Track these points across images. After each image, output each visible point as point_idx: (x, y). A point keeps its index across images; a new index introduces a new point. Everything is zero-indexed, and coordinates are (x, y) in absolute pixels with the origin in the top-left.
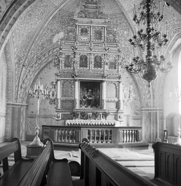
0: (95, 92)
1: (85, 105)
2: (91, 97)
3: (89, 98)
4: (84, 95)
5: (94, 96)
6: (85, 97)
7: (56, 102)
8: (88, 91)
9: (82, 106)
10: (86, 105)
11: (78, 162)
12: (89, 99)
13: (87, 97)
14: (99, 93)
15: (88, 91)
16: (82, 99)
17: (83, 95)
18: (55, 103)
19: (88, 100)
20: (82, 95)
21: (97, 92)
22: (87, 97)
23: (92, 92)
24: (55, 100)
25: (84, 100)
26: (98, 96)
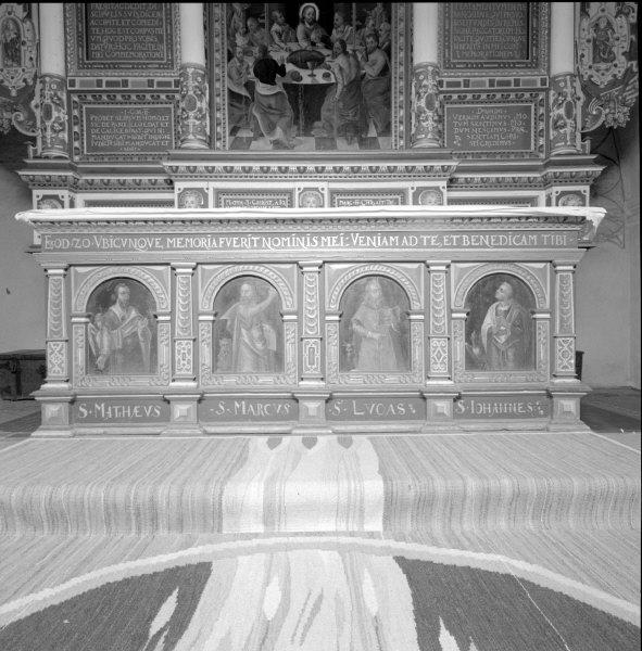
0: (348, 21)
1: (271, 128)
2: (318, 61)
3: (304, 73)
4: (265, 51)
5: (341, 60)
6: (268, 70)
7: (38, 113)
8: (292, 20)
9: (249, 140)
10: (279, 133)
11: (186, 627)
12: (307, 80)
13: (290, 67)
14: (384, 26)
15: (292, 20)
16: (249, 86)
17: (256, 50)
18: (32, 116)
19: (295, 91)
20: (246, 52)
21: (362, 19)
22: (290, 67)
23: (326, 23)
24: (27, 93)
25: (262, 89)
26: (378, 57)
